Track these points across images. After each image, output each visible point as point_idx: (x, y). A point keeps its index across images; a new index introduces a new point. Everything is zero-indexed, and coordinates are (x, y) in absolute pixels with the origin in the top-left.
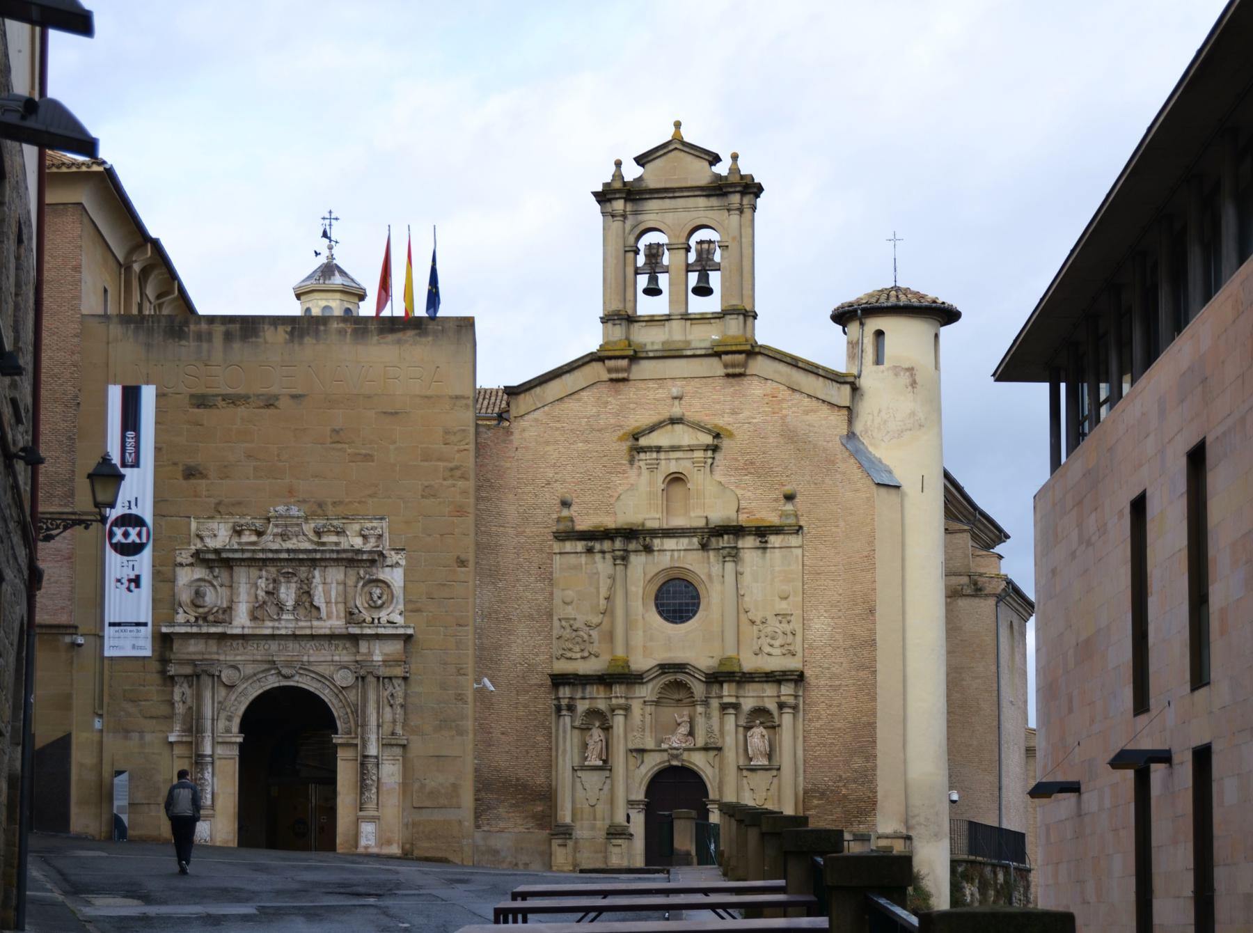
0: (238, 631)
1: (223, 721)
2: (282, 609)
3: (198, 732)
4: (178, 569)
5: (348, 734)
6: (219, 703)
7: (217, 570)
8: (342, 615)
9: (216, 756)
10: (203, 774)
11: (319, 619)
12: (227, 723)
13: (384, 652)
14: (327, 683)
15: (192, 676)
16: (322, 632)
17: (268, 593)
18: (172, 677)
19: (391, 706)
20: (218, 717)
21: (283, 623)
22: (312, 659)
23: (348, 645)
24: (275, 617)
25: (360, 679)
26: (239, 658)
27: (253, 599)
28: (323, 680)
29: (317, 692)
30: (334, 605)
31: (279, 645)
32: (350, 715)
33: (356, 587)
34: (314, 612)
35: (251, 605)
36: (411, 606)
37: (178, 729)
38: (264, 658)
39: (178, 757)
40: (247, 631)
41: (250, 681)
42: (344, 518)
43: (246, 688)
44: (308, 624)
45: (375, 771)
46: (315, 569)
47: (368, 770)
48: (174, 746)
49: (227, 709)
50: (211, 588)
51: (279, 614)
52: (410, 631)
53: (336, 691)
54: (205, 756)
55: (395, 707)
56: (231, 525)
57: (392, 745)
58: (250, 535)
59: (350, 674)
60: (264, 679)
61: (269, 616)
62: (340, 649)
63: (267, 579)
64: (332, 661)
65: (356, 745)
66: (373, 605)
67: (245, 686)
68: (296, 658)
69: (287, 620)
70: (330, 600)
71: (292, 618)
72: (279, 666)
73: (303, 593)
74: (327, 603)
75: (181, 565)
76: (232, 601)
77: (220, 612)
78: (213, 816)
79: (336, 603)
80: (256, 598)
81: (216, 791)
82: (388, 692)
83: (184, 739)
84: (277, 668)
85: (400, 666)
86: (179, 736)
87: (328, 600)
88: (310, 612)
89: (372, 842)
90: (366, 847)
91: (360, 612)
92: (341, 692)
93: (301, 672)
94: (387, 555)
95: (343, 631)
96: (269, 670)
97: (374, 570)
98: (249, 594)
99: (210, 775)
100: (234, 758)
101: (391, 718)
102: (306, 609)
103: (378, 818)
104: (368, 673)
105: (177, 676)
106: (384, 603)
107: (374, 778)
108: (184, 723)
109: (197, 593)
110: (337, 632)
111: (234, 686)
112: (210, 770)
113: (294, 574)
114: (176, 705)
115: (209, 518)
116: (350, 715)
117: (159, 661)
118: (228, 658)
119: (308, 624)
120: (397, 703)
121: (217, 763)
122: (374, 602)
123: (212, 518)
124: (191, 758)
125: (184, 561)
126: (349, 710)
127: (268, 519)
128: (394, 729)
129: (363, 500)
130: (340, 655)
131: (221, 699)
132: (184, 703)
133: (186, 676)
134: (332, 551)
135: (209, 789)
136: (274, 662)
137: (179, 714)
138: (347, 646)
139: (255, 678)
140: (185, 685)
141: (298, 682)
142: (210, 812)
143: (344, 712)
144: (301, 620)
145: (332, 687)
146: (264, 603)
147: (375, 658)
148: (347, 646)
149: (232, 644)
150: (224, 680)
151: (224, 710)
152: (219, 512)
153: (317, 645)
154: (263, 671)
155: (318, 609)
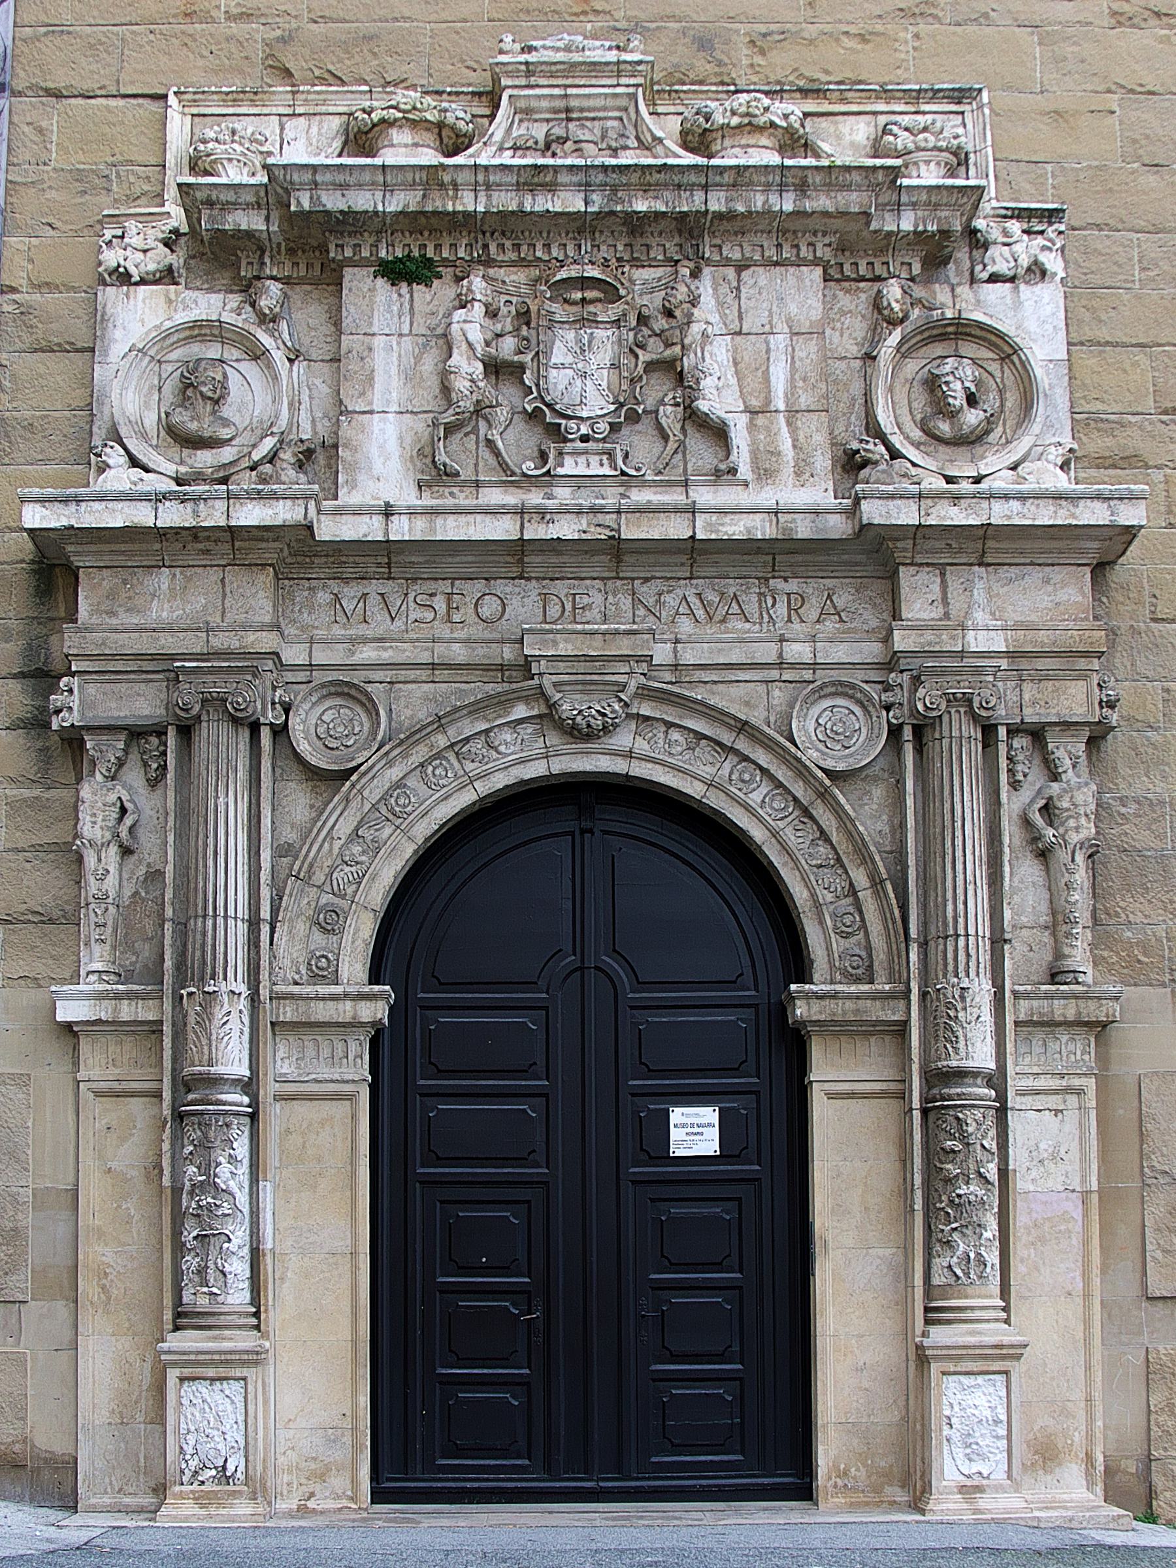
0: (370, 529)
1: (301, 927)
2: (556, 433)
3: (182, 975)
4: (111, 295)
5: (858, 980)
6: (283, 851)
7: (275, 288)
8: (823, 462)
9: (269, 1089)
10: (208, 1168)
11: (725, 474)
12: (318, 937)
13: (1012, 616)
14: (763, 758)
15: (160, 732)
16: (735, 529)
17: (495, 368)
18: (73, 740)
19: (1044, 855)
20: (275, 911)
21: (563, 494)
22: (689, 656)
23: (842, 600)
24: (529, 467)
25: (908, 733)
26: (367, 654)
27: (428, 397)
28: (742, 745)
29: (715, 801)
30: (781, 418)
31: (545, 598)
32: (866, 896)
33: (870, 357)
34: (701, 453)
35: (420, 425)
36: (1098, 444)
37: (98, 966)
38: (481, 654)
39: (98, 1094)
40: (401, 529)
41: (419, 754)
42: (805, 93)
43: (399, 784)
44: (675, 497)
45: (991, 1144)
46: (695, 274)
47: (964, 1139)
48: (84, 1045)
49: (319, 877)
50: (247, 367)
51: (543, 457)
52: (1130, 515)
53: (799, 789)
54: (215, 1081)
55: (1063, 856)
56: (336, 122)
57: (1050, 1025)
58: (416, 145)
59: (858, 720)
60: (478, 745)
61: (504, 466)
62: (811, 612)
63: (492, 313)
64: (781, 665)
65: (901, 1030)
66: (944, 427)
67: (395, 773)
68: (624, 647)
69: (579, 482)
70: (768, 401)
71: (607, 471)
72: (547, 681)
73: (650, 367)
74: (752, 412)
75: (123, 278)
76: (340, 409)
77: (287, 455)
78: (254, 1359)
79: (792, 413)
80: (446, 389)
81: (268, 1244)
82: (1026, 794)
83: (127, 1011)
84: (541, 693)
85: (1083, 675)
86: (101, 996)
87: (755, 403)
88: (681, 446)
89: (994, 1467)
90: (970, 1490)
91: (895, 454)
92: (823, 795)
93: (646, 710)
94: (995, 234)
95: (837, 526)
96: (503, 702)
97: (942, 294)
98: (410, 377)
99: (244, 1170)
100: (351, 1098)
101: (1044, 907)
102: (665, 438)
103: (1014, 1352)
104: (951, 699)
105: (89, 729)
106: (990, 422)
107: (991, 1170)
108: (124, 942)
109: (188, 388)
110: (803, 529)
111: (346, 774)
112: (242, 1148)
113: (611, 293)
114: (90, 860)
115: (234, 98)
116: (866, 896)
117: (22, 675)
118: (321, 656)
119: (675, 497)
120: (1074, 838)
121: (275, 1116)
122: (952, 415)
123: (256, 95)
124: (158, 1095)
125: (137, 264)
126: (860, 877)
127: (492, 98)
128: (1059, 955)
129: (879, 28)
130: (813, 639)
131: (289, 835)
132: (126, 851)
133: (135, 733)
134: (781, 179)
135: (239, 1236)
136: (525, 667)
137: (102, 898)
138: (840, 601)
139: (441, 741)
140: (134, 776)
141: (630, 755)
142: (244, 1341)
143: (840, 884)
144: (643, 484)
145: (782, 773)
146: (479, 410)
147: (977, 641)
148: (842, 600)
149: (337, 598)
150: (303, 747)
151: (305, 880)
152: (288, 73)
153: (712, 597)
154: (476, 709)
155: (719, 433)
